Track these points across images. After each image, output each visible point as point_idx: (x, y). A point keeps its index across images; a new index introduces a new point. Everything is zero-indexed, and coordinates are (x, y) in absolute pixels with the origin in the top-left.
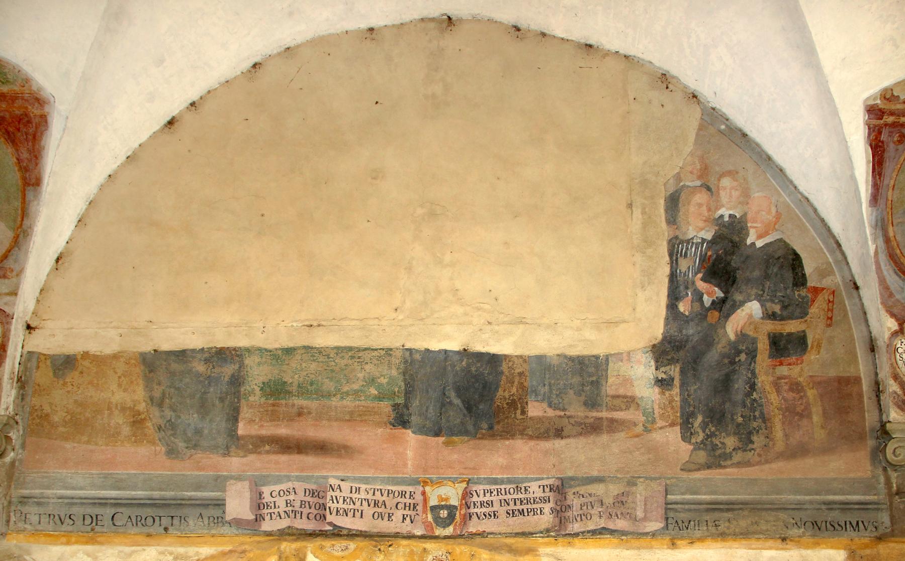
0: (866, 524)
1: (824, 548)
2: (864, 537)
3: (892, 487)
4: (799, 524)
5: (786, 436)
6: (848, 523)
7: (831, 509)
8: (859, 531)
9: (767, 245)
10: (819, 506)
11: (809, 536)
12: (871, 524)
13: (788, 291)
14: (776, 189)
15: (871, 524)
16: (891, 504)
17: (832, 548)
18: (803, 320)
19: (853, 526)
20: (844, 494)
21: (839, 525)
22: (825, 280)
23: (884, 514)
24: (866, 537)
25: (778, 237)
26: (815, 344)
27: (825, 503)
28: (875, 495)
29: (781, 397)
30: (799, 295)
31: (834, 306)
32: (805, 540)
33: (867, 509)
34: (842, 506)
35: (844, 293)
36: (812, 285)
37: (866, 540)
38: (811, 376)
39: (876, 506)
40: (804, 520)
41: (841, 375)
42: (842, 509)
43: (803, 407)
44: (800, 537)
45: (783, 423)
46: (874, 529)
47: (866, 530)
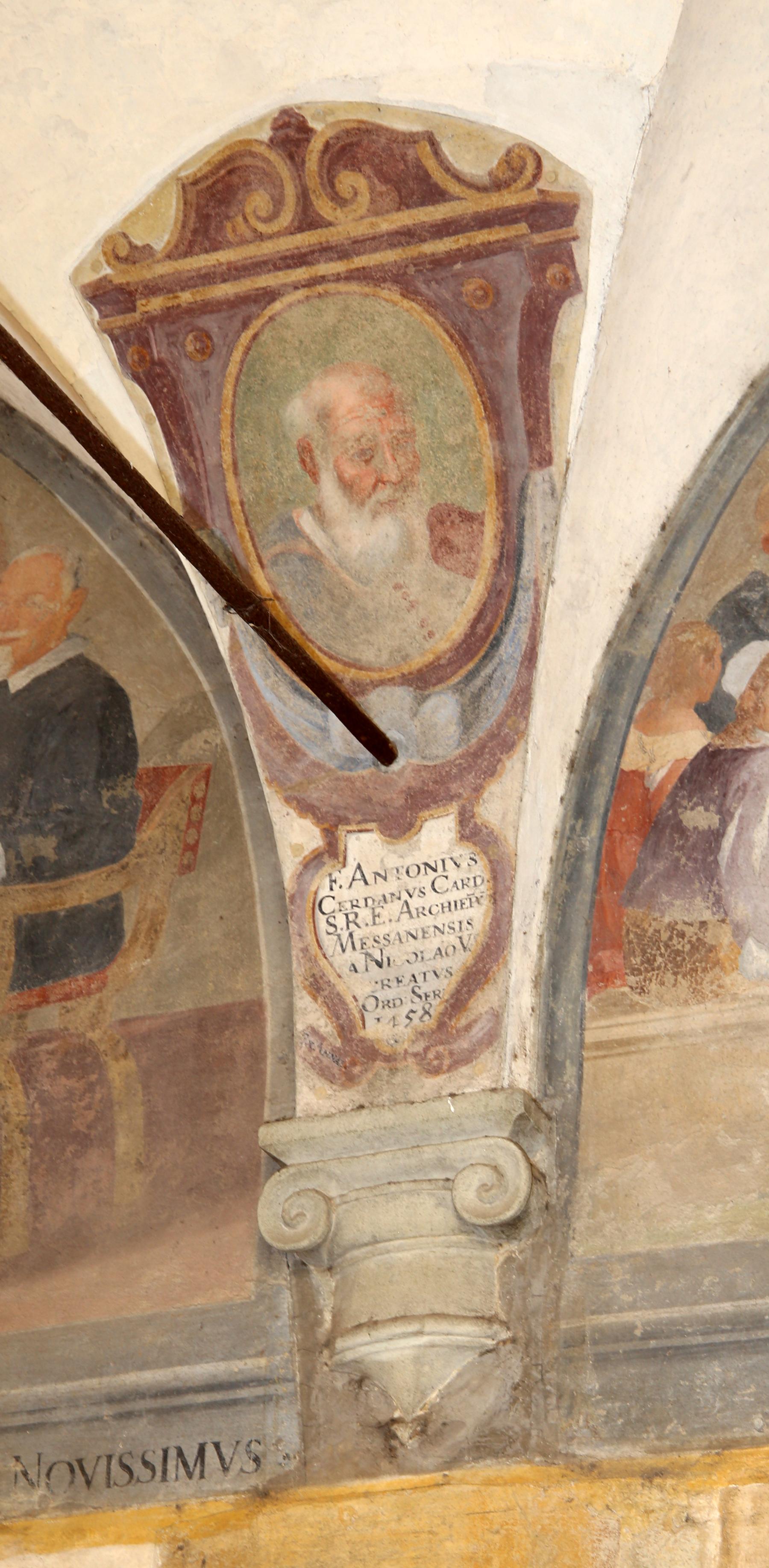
0: (226, 1452)
1: (97, 1545)
2: (217, 1493)
3: (318, 1323)
4: (32, 1474)
5: (36, 1206)
6: (172, 1453)
7: (129, 1415)
8: (202, 1476)
9: (38, 681)
10: (92, 1411)
11: (56, 1508)
12: (242, 1448)
13: (84, 795)
14: (80, 530)
15: (242, 1448)
16: (309, 1375)
17: (118, 1540)
18: (116, 866)
19: (185, 1464)
20: (169, 1364)
21: (146, 1464)
22: (185, 744)
23: (283, 1413)
24: (224, 1492)
25: (71, 654)
26: (144, 926)
27: (111, 1400)
28: (261, 1354)
29: (33, 1095)
30: (112, 801)
31: (206, 813)
32: (45, 1521)
33: (235, 1402)
34: (160, 1403)
35: (235, 772)
36: (151, 765)
37: (222, 1505)
38: (124, 1022)
39: (260, 1391)
40: (48, 1460)
41: (207, 1004)
42: (160, 1412)
43: (91, 1115)
44: (31, 1514)
45: (33, 1171)
46: (252, 1466)
47: (225, 1469)
